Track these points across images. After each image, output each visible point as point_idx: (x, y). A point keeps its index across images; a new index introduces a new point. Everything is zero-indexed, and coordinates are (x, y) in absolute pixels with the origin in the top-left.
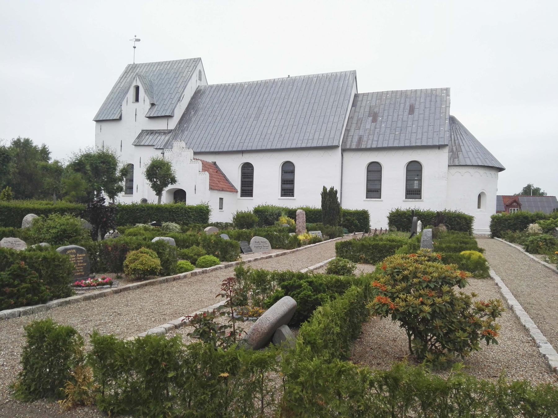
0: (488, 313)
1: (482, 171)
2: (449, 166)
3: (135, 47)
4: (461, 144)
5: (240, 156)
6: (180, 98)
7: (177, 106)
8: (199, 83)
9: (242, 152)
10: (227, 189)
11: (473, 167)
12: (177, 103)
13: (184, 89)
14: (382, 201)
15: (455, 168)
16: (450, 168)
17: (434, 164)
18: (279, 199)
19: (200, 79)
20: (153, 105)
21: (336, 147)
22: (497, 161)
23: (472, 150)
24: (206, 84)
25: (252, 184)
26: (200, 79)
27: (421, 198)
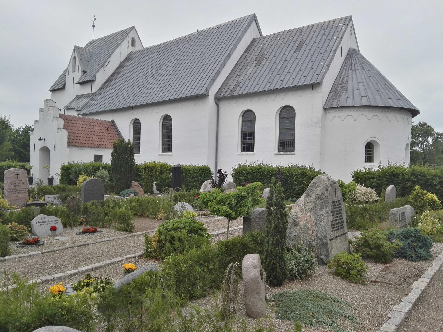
0: (224, 323)
1: (369, 114)
2: (325, 109)
3: (93, 26)
4: (350, 81)
5: (130, 112)
6: (104, 63)
7: (100, 71)
8: (131, 49)
9: (132, 108)
10: (86, 145)
11: (371, 110)
12: (100, 69)
13: (111, 55)
14: (254, 155)
15: (333, 111)
16: (327, 112)
17: (307, 108)
18: (160, 155)
19: (133, 45)
20: (85, 72)
21: (202, 97)
22: (406, 100)
23: (372, 88)
24: (141, 48)
25: (254, 136)
26: (133, 45)
27: (294, 151)
